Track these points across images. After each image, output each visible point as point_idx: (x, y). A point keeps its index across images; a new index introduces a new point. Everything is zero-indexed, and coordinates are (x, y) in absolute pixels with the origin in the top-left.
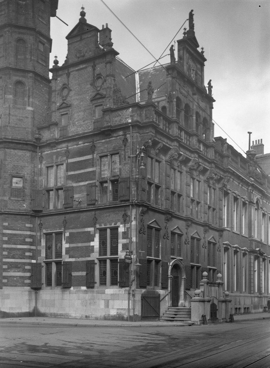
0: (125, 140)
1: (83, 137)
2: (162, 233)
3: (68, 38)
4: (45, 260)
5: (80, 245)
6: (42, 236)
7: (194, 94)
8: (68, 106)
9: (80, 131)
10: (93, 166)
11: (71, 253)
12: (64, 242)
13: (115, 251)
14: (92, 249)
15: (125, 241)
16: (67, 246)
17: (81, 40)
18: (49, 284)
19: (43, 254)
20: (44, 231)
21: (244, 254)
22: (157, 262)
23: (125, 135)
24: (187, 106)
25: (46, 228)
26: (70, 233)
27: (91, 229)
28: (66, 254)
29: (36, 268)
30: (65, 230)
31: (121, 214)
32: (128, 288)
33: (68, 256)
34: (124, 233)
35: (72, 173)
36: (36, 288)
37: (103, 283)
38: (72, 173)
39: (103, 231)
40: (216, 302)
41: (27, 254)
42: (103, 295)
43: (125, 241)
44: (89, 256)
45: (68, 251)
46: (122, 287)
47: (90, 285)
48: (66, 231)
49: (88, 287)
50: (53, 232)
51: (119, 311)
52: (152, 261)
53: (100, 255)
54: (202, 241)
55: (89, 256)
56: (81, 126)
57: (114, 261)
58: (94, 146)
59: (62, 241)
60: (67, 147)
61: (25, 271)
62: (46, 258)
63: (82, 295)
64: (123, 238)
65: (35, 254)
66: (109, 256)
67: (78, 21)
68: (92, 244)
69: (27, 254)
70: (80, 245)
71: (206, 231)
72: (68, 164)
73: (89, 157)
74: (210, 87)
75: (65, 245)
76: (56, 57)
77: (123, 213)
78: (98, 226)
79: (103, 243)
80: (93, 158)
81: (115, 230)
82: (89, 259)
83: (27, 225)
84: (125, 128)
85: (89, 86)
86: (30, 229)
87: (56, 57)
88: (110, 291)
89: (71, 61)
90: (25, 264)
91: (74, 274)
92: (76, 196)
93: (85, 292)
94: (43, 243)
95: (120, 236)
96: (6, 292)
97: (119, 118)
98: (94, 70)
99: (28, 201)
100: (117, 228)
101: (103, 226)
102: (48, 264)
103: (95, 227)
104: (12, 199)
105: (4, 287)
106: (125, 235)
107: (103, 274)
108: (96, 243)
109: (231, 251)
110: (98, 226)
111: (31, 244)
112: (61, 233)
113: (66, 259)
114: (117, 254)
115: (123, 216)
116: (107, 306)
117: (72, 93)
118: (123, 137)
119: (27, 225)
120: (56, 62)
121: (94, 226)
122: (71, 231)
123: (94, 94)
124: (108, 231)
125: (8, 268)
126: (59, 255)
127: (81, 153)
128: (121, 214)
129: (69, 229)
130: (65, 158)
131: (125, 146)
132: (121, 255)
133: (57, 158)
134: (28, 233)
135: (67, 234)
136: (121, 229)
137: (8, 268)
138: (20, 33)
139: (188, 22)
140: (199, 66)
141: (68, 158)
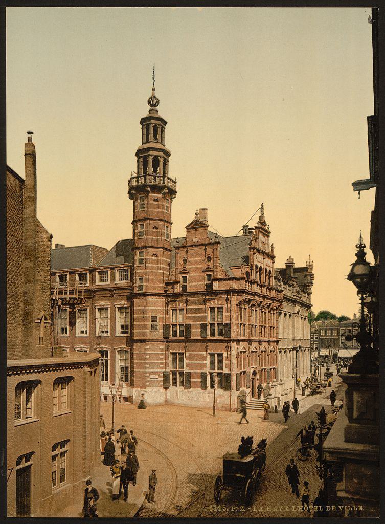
6: (169, 354)
7: (264, 259)
12: (185, 359)
13: (220, 367)
16: (188, 361)
18: (175, 384)
20: (171, 351)
21: (290, 351)
22: (245, 372)
28: (187, 366)
29: (166, 376)
32: (229, 392)
35: (190, 315)
38: (190, 315)
39: (212, 355)
40: (280, 396)
50: (177, 353)
57: (220, 375)
64: (226, 360)
68: (205, 362)
71: (269, 345)
74: (272, 247)
75: (186, 362)
78: (209, 351)
79: (212, 361)
81: (220, 355)
82: (202, 371)
86: (162, 350)
90: (160, 372)
91: (192, 380)
94: (170, 358)
101: (212, 352)
103: (206, 351)
107: (212, 382)
108: (208, 362)
109: (283, 351)
110: (209, 351)
112: (183, 354)
113: (186, 370)
124: (216, 355)
130: (185, 305)
132: (225, 371)
133: (179, 304)
135: (187, 354)
136: (225, 355)
139: (260, 210)
140: (267, 238)
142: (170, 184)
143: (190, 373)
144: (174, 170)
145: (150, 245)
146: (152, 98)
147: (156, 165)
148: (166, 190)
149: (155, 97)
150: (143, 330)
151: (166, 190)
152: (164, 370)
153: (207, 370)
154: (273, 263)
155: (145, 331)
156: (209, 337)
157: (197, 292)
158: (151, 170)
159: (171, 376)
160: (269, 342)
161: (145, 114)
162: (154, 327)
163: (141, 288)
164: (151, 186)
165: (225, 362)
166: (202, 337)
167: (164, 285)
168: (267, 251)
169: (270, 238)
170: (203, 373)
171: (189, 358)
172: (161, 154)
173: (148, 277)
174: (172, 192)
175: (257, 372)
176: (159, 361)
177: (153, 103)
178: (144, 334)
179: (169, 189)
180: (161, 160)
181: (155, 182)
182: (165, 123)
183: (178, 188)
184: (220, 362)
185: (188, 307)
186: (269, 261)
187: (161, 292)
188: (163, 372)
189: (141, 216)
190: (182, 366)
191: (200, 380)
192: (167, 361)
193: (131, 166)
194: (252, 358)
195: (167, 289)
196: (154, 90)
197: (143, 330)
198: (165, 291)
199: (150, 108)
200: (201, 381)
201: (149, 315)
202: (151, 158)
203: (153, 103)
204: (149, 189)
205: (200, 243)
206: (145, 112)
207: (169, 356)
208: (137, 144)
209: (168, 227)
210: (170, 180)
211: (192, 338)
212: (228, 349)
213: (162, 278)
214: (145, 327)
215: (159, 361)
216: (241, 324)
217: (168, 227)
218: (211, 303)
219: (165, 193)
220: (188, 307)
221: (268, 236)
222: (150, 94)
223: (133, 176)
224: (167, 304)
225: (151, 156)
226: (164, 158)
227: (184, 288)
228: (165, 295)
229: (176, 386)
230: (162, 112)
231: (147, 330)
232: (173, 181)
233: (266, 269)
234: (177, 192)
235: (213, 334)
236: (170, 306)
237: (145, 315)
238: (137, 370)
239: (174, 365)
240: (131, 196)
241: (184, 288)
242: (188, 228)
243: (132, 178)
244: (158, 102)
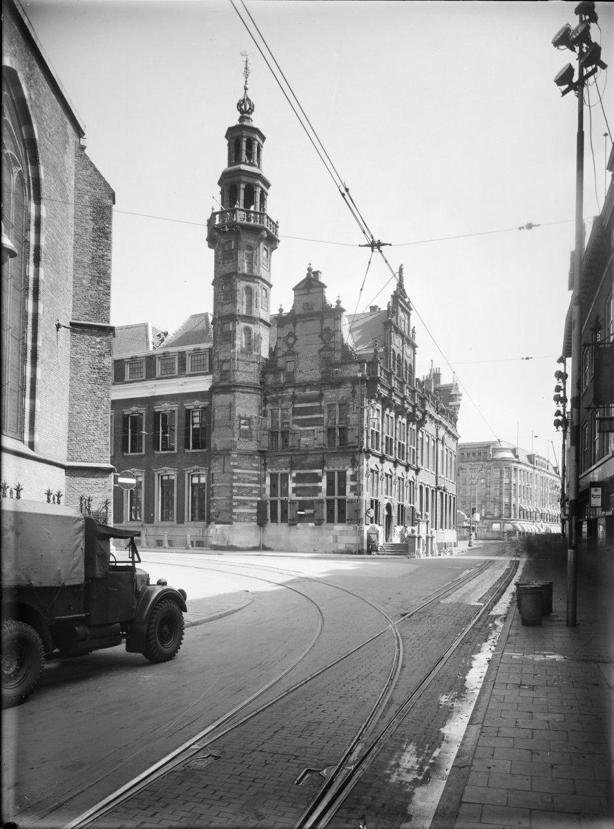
0: (354, 392)
1: (309, 385)
3: (295, 289)
5: (307, 485)
8: (294, 354)
9: (308, 379)
10: (321, 413)
11: (298, 492)
14: (319, 489)
15: (353, 483)
17: (309, 293)
18: (274, 519)
19: (268, 492)
23: (354, 387)
24: (399, 355)
26: (297, 474)
27: (319, 471)
28: (293, 492)
29: (261, 506)
30: (291, 470)
31: (349, 460)
34: (352, 476)
36: (261, 523)
37: (330, 520)
39: (330, 476)
41: (254, 492)
42: (332, 531)
43: (353, 483)
44: (317, 496)
45: (294, 490)
46: (349, 524)
47: (319, 523)
48: (293, 471)
49: (316, 524)
51: (348, 546)
53: (327, 495)
54: (405, 481)
55: (317, 496)
56: (308, 375)
58: (323, 395)
59: (288, 480)
60: (294, 393)
61: (252, 507)
62: (271, 496)
63: (309, 532)
64: (352, 480)
65: (262, 491)
66: (336, 496)
67: (305, 276)
68: (320, 484)
69: (254, 492)
70: (307, 485)
72: (293, 408)
73: (317, 404)
75: (291, 485)
76: (281, 305)
77: (351, 458)
78: (326, 468)
79: (330, 484)
80: (321, 406)
81: (342, 475)
82: (316, 498)
83: (254, 465)
84: (355, 381)
85: (318, 338)
86: (257, 469)
87: (281, 305)
88: (338, 527)
89: (297, 312)
90: (252, 501)
92: (303, 439)
93: (313, 528)
94: (268, 480)
95: (348, 478)
96: (236, 528)
97: (348, 371)
98: (322, 323)
99: (254, 443)
100: (345, 472)
101: (331, 469)
102: (274, 503)
103: (323, 469)
104: (241, 439)
105: (234, 523)
106: (353, 478)
108: (323, 484)
111: (257, 482)
114: (345, 494)
115: (351, 461)
116: (336, 540)
117: (298, 342)
118: (351, 389)
119: (254, 465)
120: (281, 310)
121: (322, 467)
122: (298, 471)
123: (322, 346)
124: (336, 474)
125: (238, 505)
126: (285, 493)
127: (308, 400)
128: (349, 460)
129: (296, 469)
130: (291, 403)
131: (354, 397)
133: (283, 402)
134: (255, 472)
135: (294, 475)
136: (350, 472)
137: (238, 505)
138: (247, 281)
141: (294, 403)
144: (275, 206)
146: (243, 101)
147: (249, 201)
149: (248, 99)
152: (259, 499)
153: (323, 495)
158: (240, 204)
160: (407, 467)
161: (235, 122)
165: (349, 484)
174: (272, 241)
176: (253, 485)
177: (245, 108)
182: (263, 138)
183: (281, 234)
185: (296, 406)
188: (258, 502)
192: (263, 486)
193: (212, 200)
196: (246, 89)
203: (245, 108)
207: (267, 478)
208: (222, 164)
210: (271, 220)
215: (253, 485)
220: (296, 406)
223: (215, 211)
226: (261, 188)
227: (290, 375)
230: (256, 121)
232: (273, 223)
234: (279, 241)
238: (218, 498)
240: (212, 241)
243: (214, 214)
244: (252, 110)
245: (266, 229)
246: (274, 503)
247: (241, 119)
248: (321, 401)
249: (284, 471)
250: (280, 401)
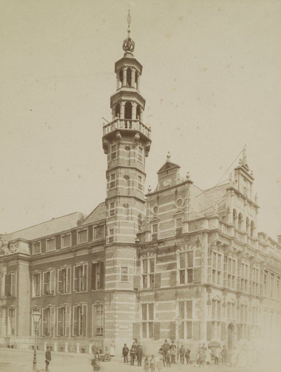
2: (222, 303)
4: (142, 321)
25: (143, 301)
26: (159, 304)
28: (156, 317)
33: (157, 318)
52: (215, 322)
75: (155, 312)
91: (162, 330)
113: (155, 320)
130: (155, 254)
142: (145, 132)
143: (159, 323)
145: (121, 194)
148: (137, 136)
150: (112, 282)
151: (137, 136)
154: (257, 213)
155: (114, 281)
156: (178, 284)
157: (167, 238)
159: (141, 328)
162: (125, 278)
163: (111, 239)
164: (121, 132)
165: (195, 309)
166: (171, 285)
167: (136, 237)
168: (249, 198)
169: (253, 185)
170: (172, 322)
171: (159, 308)
172: (134, 99)
173: (118, 227)
175: (235, 325)
177: (128, 46)
178: (113, 285)
179: (141, 135)
180: (134, 106)
181: (126, 127)
184: (190, 309)
185: (159, 256)
186: (252, 211)
187: (133, 243)
189: (113, 165)
190: (151, 317)
191: (168, 330)
194: (229, 310)
195: (138, 240)
197: (112, 282)
198: (136, 242)
199: (124, 52)
200: (170, 331)
201: (118, 266)
202: (124, 103)
203: (128, 46)
204: (119, 135)
205: (171, 186)
206: (120, 54)
209: (141, 178)
210: (143, 126)
211: (162, 287)
212: (198, 294)
213: (133, 228)
214: (114, 278)
216: (214, 271)
217: (141, 178)
218: (181, 250)
219: (136, 140)
220: (159, 256)
221: (251, 183)
222: (125, 37)
224: (139, 255)
225: (124, 101)
226: (137, 103)
227: (155, 236)
228: (136, 245)
229: (146, 337)
230: (137, 55)
231: (117, 281)
232: (146, 128)
233: (247, 218)
235: (182, 281)
236: (141, 257)
237: (115, 266)
239: (145, 317)
241: (155, 236)
242: (160, 173)
245: (139, 132)
246: (144, 324)
247: (125, 54)
248: (175, 251)
249: (151, 302)
250: (148, 253)
